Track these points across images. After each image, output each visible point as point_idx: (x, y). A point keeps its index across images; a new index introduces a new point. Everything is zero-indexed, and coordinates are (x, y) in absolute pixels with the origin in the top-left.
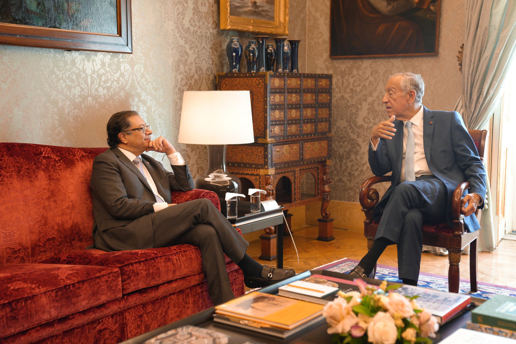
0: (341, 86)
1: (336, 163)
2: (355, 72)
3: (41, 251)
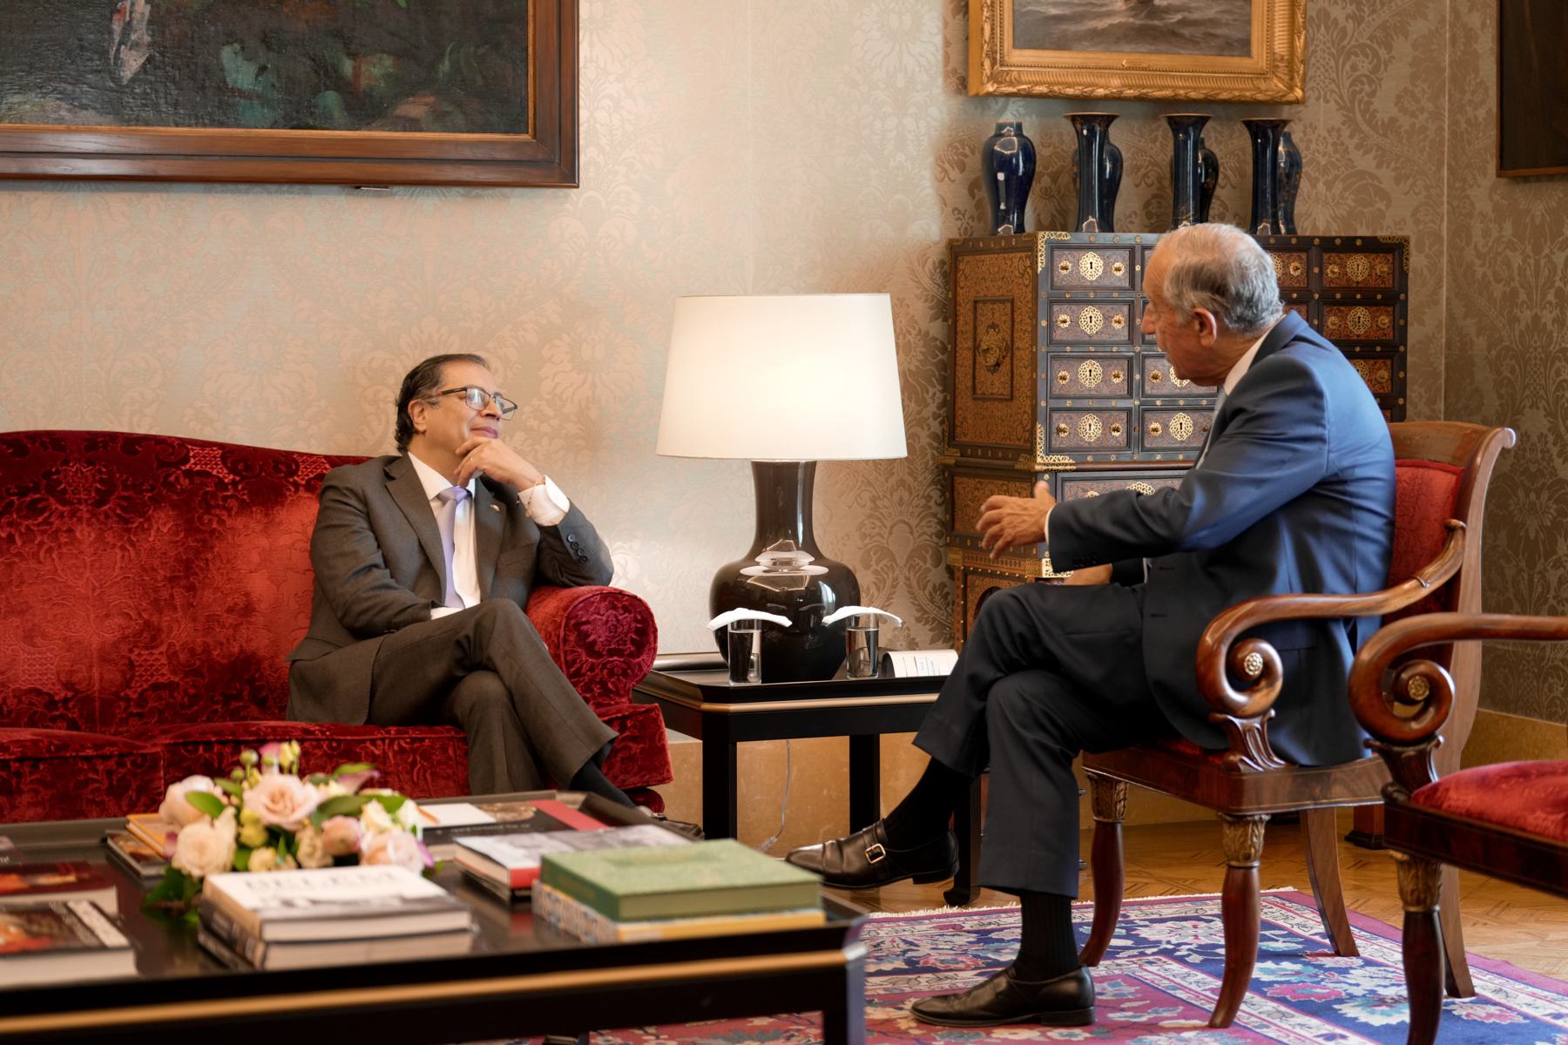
0: (1532, 280)
1: (1520, 571)
3: (132, 715)
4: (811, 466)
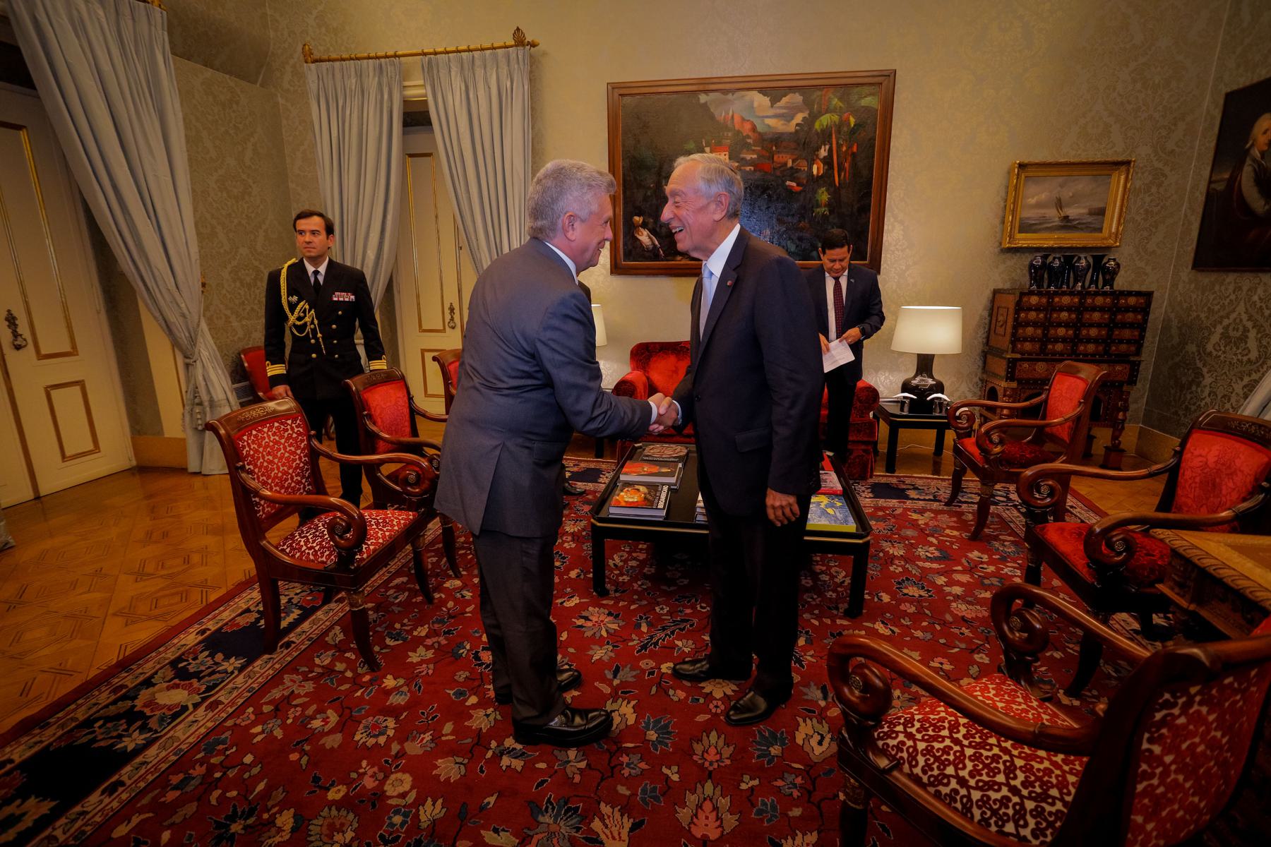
2: (1217, 288)
4: (932, 356)
